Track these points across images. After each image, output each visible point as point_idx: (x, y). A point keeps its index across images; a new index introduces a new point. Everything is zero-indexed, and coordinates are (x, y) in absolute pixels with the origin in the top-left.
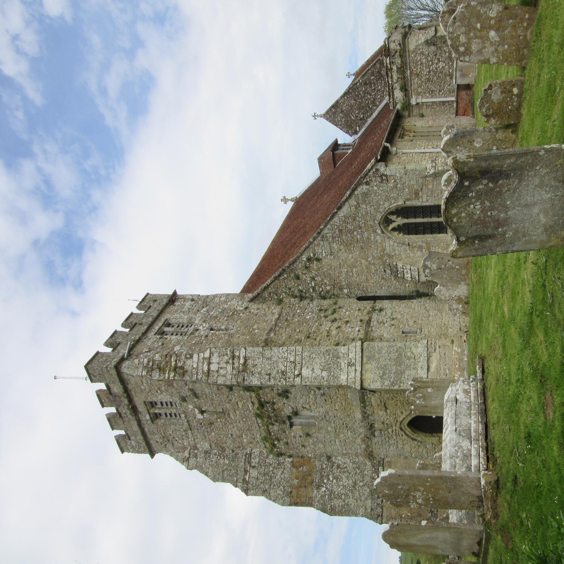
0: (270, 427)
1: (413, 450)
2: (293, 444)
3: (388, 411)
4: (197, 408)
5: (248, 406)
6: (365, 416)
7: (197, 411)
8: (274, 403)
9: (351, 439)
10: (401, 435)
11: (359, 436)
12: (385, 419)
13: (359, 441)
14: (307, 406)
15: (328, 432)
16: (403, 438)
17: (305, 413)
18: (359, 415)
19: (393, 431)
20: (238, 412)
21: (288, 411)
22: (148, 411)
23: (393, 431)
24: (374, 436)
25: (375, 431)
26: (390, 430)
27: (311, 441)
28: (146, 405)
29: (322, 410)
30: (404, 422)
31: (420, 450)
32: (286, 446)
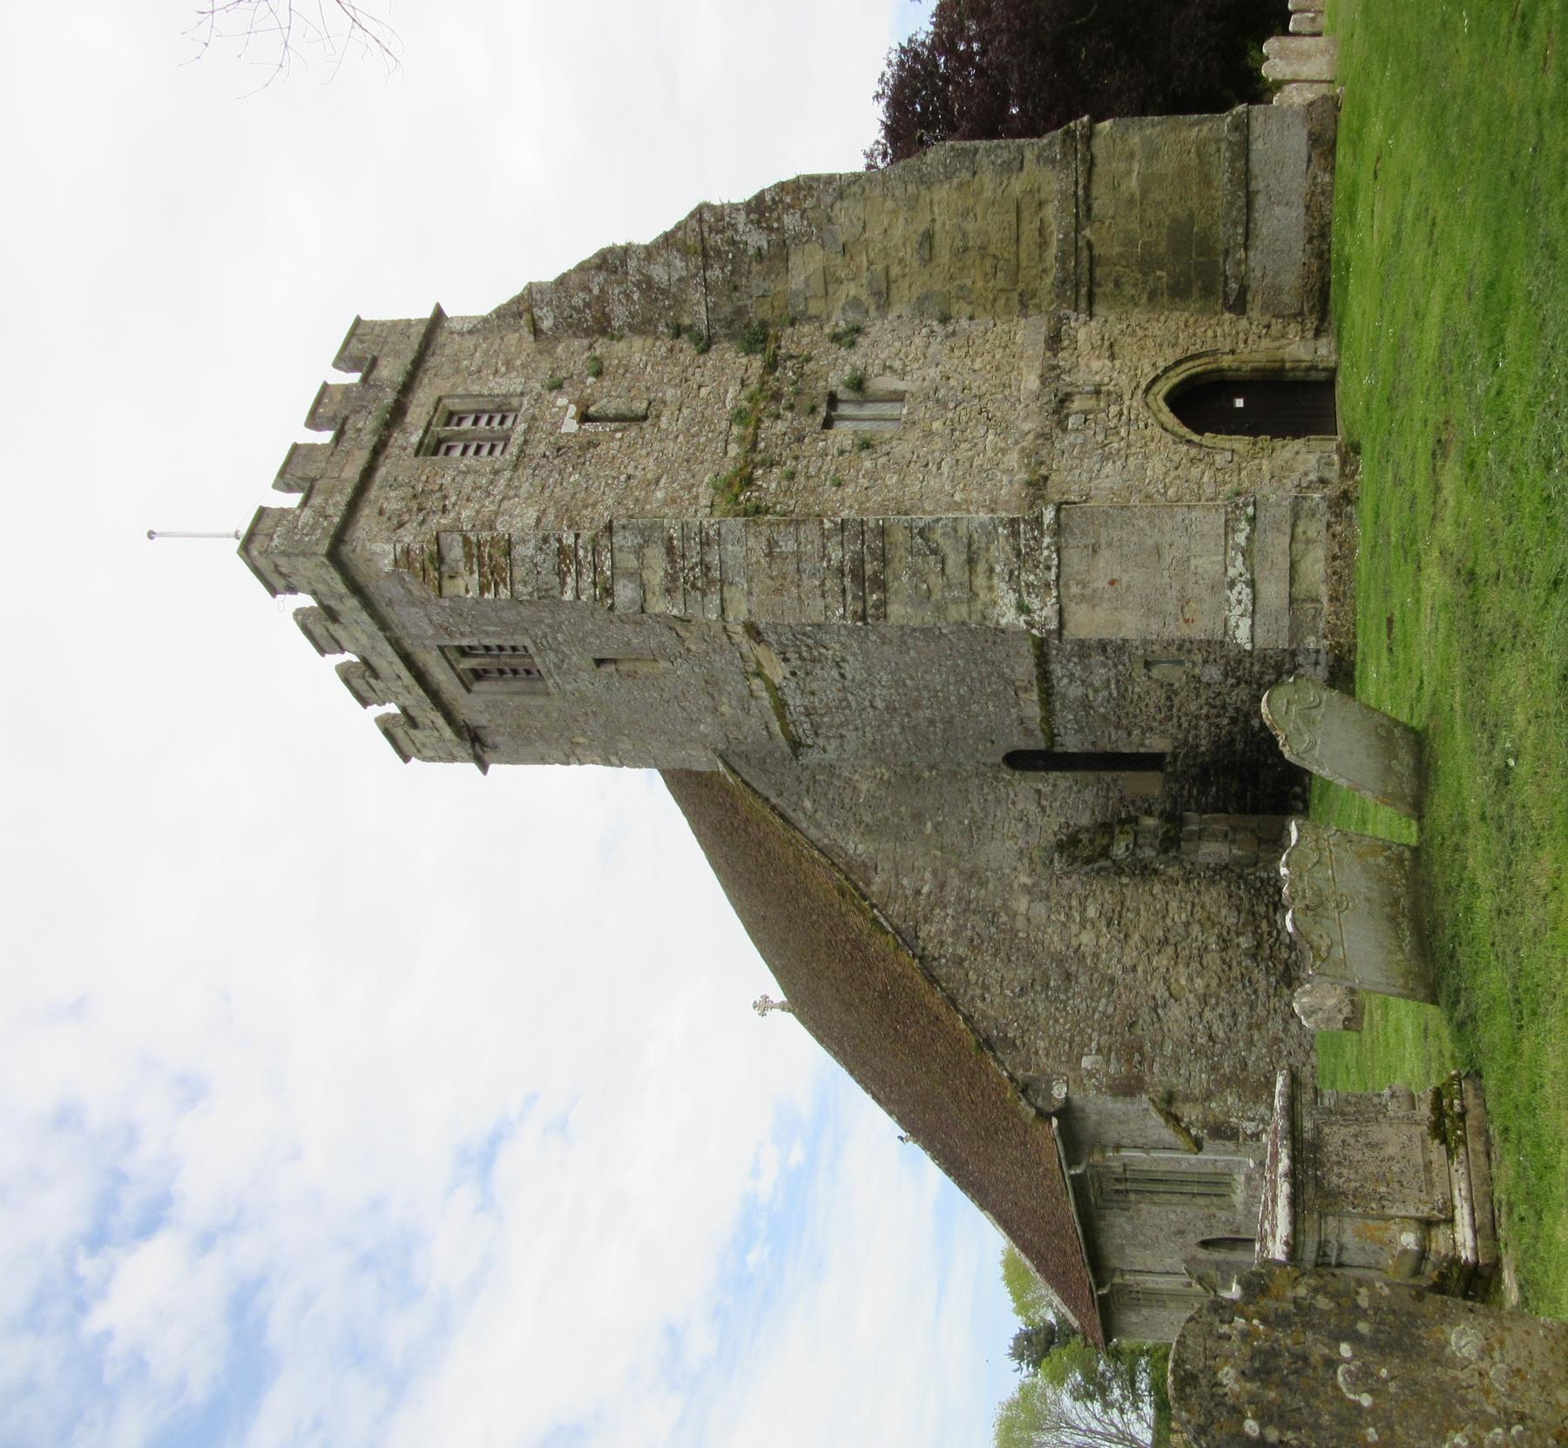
0: (767, 423)
1: (1173, 474)
2: (808, 478)
3: (1117, 363)
4: (577, 403)
5: (726, 391)
6: (1051, 374)
7: (573, 410)
8: (808, 359)
9: (989, 454)
10: (1142, 425)
11: (1017, 442)
12: (1106, 380)
13: (1013, 459)
14: (897, 365)
15: (928, 435)
16: (1148, 432)
17: (883, 383)
18: (1032, 382)
19: (1121, 414)
20: (685, 411)
21: (836, 380)
22: (429, 423)
23: (1121, 414)
24: (1064, 430)
25: (1067, 417)
26: (1114, 409)
27: (868, 464)
28: (436, 410)
29: (933, 372)
30: (1155, 389)
31: (1195, 472)
32: (785, 483)
